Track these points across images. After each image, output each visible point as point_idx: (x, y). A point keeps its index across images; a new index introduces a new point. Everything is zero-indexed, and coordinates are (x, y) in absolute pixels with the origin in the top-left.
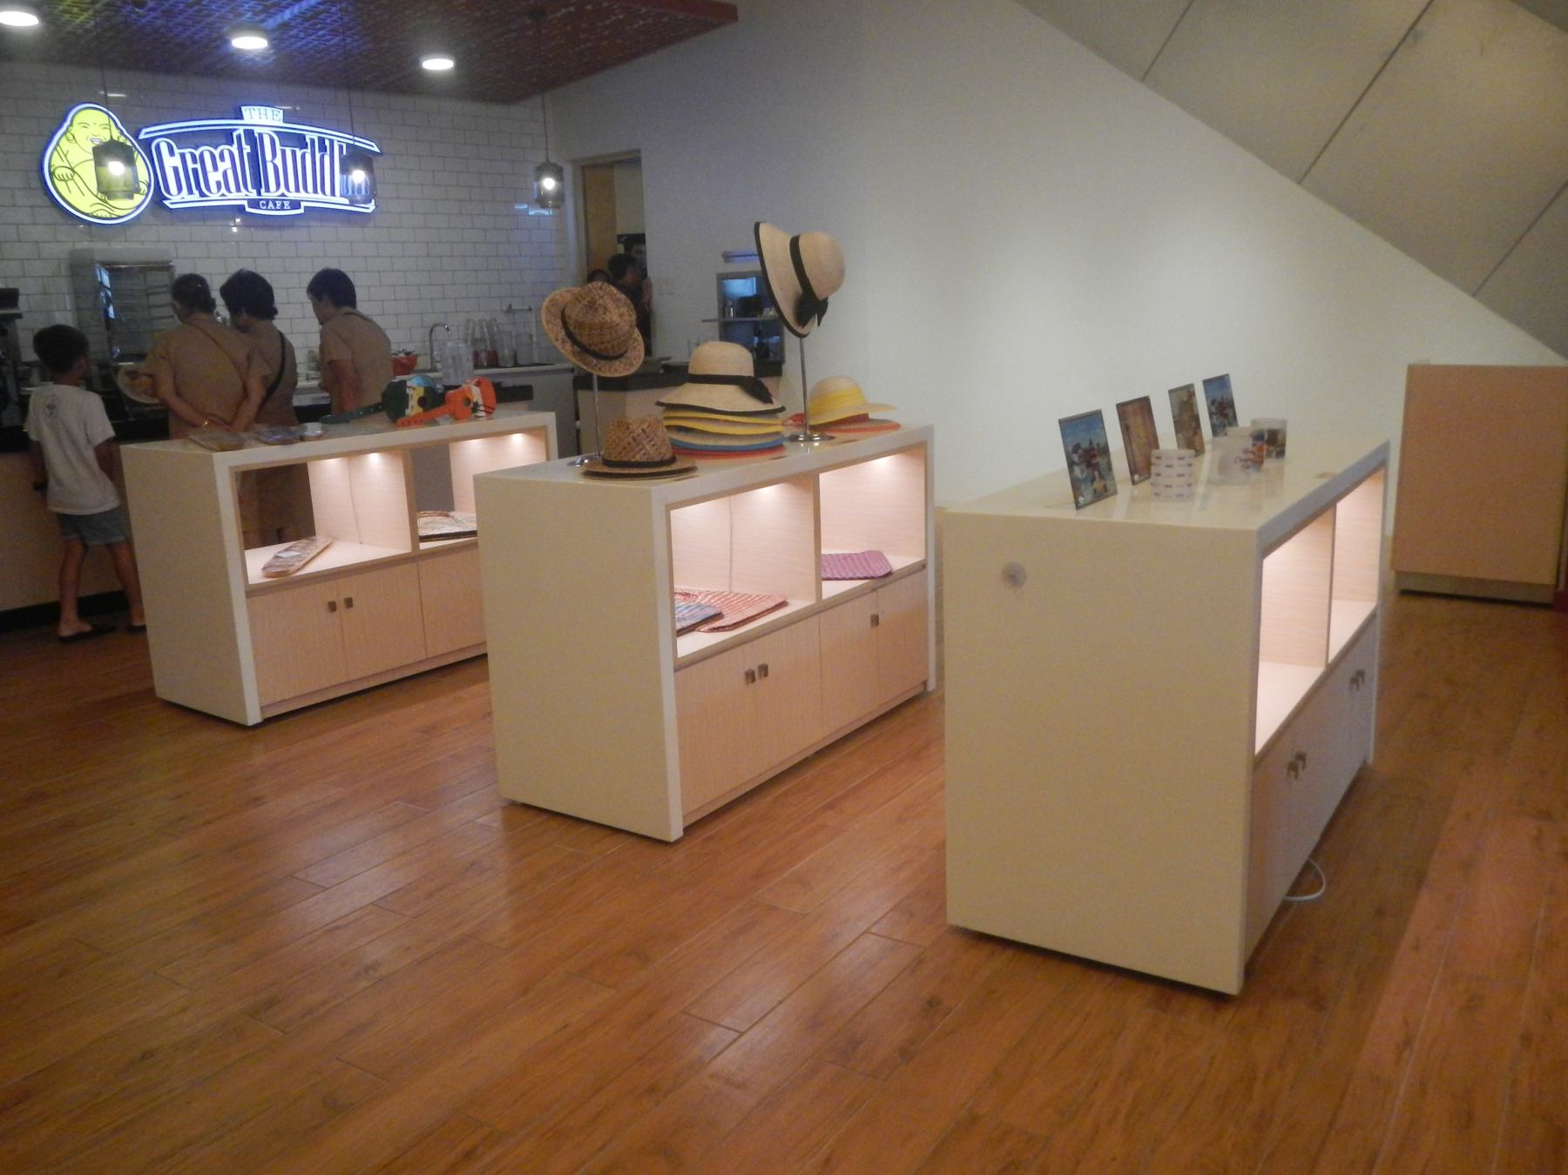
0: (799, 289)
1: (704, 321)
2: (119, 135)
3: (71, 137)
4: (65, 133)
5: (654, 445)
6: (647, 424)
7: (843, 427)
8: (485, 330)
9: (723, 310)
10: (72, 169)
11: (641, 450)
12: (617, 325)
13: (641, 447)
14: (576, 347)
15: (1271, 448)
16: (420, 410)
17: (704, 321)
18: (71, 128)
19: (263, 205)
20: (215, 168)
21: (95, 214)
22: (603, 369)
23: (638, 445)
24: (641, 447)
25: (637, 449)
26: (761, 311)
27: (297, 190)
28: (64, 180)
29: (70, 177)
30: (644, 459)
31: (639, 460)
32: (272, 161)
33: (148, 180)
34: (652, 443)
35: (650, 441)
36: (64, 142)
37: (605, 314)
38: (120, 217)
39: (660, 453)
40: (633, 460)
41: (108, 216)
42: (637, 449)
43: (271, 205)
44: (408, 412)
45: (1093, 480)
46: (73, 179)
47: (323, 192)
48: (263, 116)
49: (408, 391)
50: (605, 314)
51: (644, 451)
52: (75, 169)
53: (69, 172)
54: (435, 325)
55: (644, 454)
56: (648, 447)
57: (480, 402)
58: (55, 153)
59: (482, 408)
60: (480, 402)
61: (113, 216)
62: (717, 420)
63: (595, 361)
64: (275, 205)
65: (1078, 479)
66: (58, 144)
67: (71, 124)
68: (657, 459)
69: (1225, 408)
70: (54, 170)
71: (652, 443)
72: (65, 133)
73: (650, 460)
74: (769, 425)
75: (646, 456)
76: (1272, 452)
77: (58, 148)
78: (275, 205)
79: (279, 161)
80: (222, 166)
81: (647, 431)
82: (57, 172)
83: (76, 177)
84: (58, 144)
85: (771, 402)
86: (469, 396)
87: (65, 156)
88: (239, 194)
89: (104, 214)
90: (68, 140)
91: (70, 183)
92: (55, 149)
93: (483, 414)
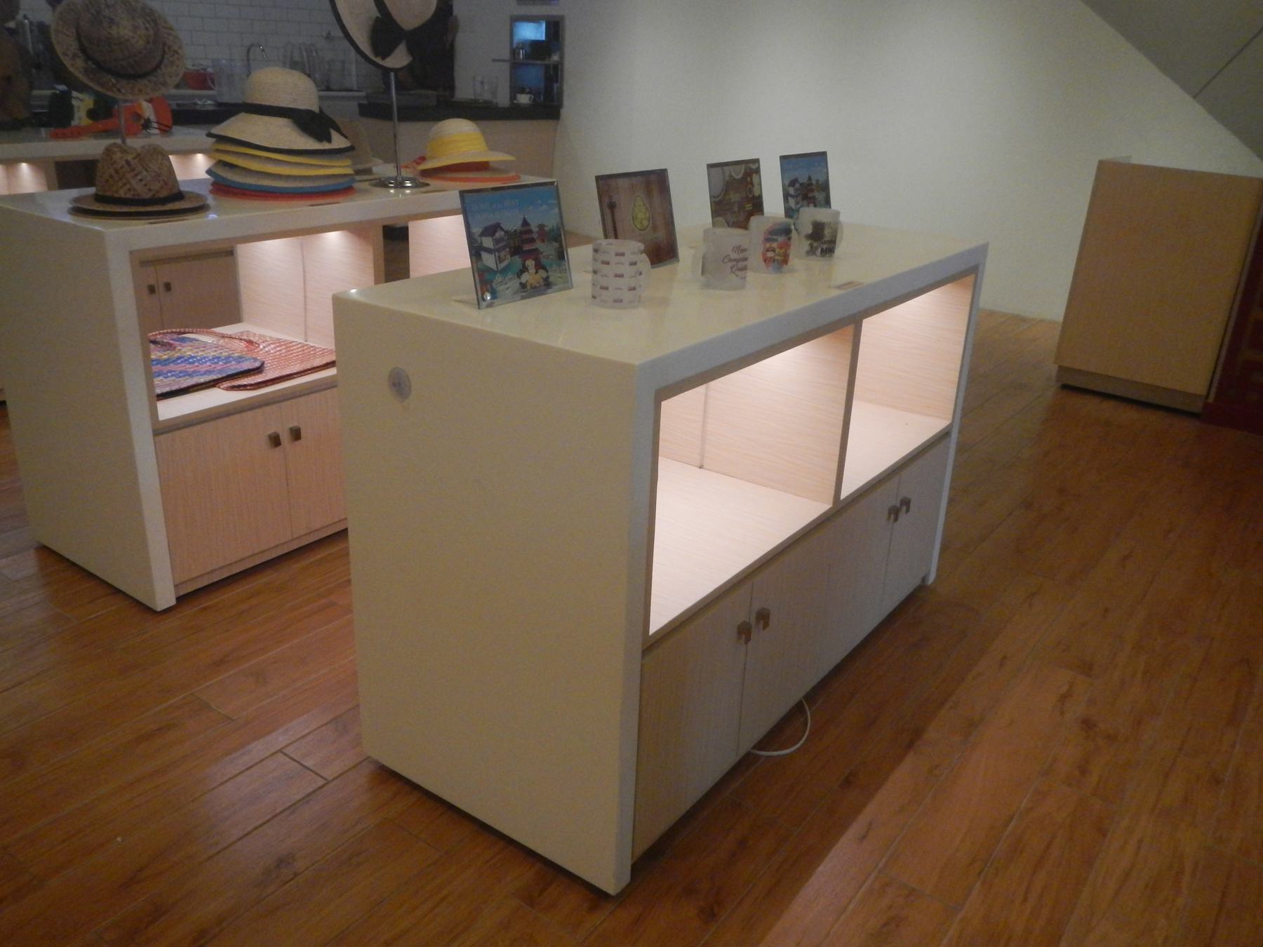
0: (375, 13)
1: (494, 60)
5: (141, 180)
6: (134, 155)
7: (449, 175)
8: (304, 54)
9: (514, 52)
11: (125, 184)
12: (128, 40)
13: (124, 181)
14: (90, 63)
15: (815, 244)
16: (89, 122)
17: (494, 60)
22: (123, 91)
23: (121, 179)
24: (124, 181)
25: (120, 184)
26: (550, 56)
30: (129, 196)
31: (123, 196)
34: (139, 177)
35: (137, 175)
37: (110, 27)
39: (150, 190)
40: (116, 195)
42: (120, 184)
44: (75, 123)
45: (524, 269)
49: (74, 102)
50: (110, 27)
51: (128, 186)
54: (252, 45)
55: (129, 190)
56: (133, 182)
57: (153, 118)
59: (155, 125)
60: (153, 118)
62: (270, 159)
63: (113, 81)
65: (489, 270)
68: (148, 196)
69: (812, 191)
71: (139, 177)
73: (137, 197)
74: (327, 167)
75: (132, 192)
76: (816, 248)
81: (133, 163)
85: (329, 140)
86: (139, 112)
93: (157, 131)
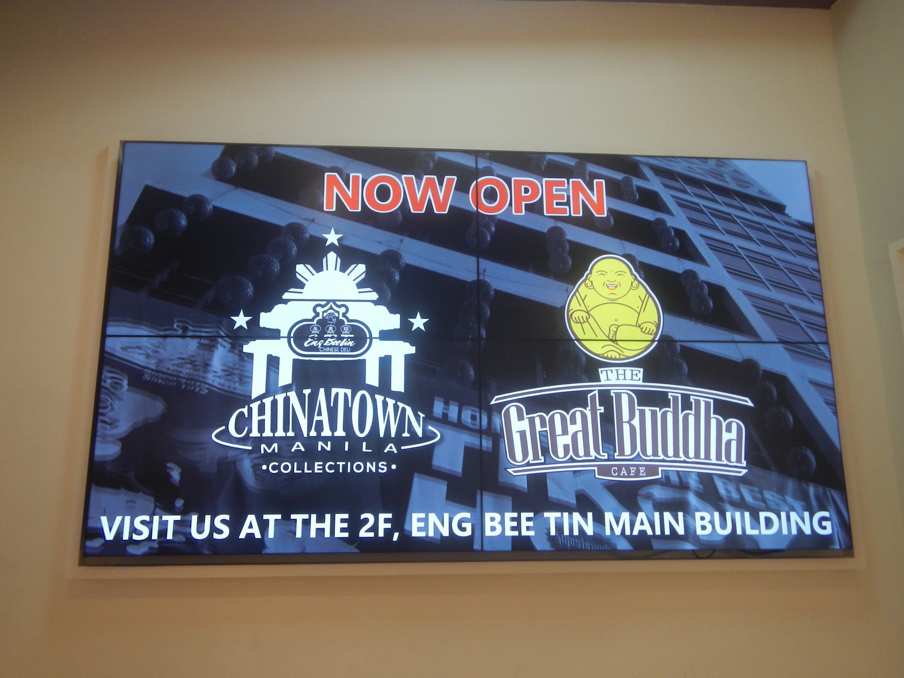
2: (633, 280)
3: (589, 284)
4: (585, 280)
10: (588, 312)
18: (590, 275)
21: (605, 355)
28: (581, 323)
29: (586, 320)
33: (657, 322)
36: (583, 290)
38: (628, 358)
41: (618, 357)
46: (587, 321)
52: (590, 313)
58: (575, 297)
61: (622, 357)
66: (577, 290)
67: (591, 272)
70: (572, 314)
72: (585, 280)
77: (577, 294)
82: (575, 315)
83: (591, 320)
84: (577, 290)
87: (583, 301)
89: (614, 355)
90: (586, 286)
91: (586, 325)
92: (574, 294)
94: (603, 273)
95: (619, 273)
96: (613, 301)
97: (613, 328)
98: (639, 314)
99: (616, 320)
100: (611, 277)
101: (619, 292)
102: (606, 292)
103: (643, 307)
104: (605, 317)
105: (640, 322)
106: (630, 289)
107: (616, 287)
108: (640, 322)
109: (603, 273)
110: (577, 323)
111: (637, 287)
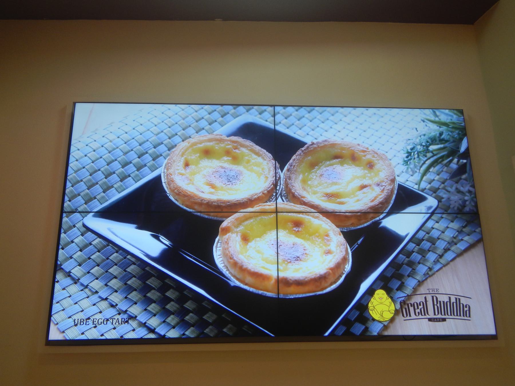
3: (374, 298)
10: (374, 307)
19: (433, 320)
20: (418, 308)
27: (445, 315)
32: (436, 305)
43: (435, 320)
47: (454, 315)
48: (433, 291)
53: (373, 308)
64: (437, 320)
78: (437, 320)
79: (439, 305)
80: (420, 307)
83: (375, 310)
88: (425, 316)
90: (373, 299)
91: (373, 311)
94: (378, 294)
95: (383, 294)
96: (381, 303)
97: (382, 312)
98: (389, 307)
99: (382, 309)
100: (381, 296)
101: (383, 300)
102: (379, 300)
103: (390, 305)
104: (379, 308)
105: (389, 310)
106: (386, 299)
107: (382, 299)
108: (389, 310)
109: (378, 294)
110: (371, 310)
111: (389, 299)
